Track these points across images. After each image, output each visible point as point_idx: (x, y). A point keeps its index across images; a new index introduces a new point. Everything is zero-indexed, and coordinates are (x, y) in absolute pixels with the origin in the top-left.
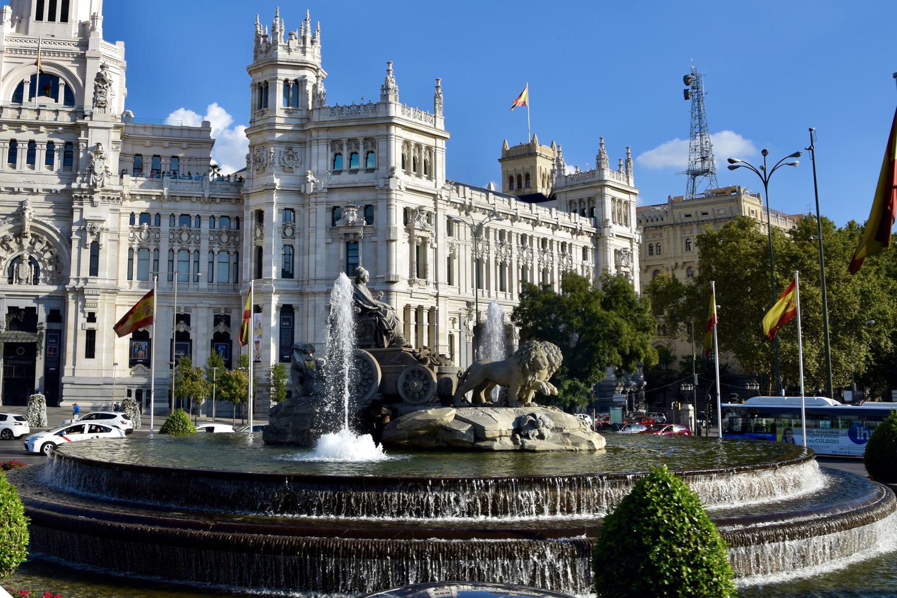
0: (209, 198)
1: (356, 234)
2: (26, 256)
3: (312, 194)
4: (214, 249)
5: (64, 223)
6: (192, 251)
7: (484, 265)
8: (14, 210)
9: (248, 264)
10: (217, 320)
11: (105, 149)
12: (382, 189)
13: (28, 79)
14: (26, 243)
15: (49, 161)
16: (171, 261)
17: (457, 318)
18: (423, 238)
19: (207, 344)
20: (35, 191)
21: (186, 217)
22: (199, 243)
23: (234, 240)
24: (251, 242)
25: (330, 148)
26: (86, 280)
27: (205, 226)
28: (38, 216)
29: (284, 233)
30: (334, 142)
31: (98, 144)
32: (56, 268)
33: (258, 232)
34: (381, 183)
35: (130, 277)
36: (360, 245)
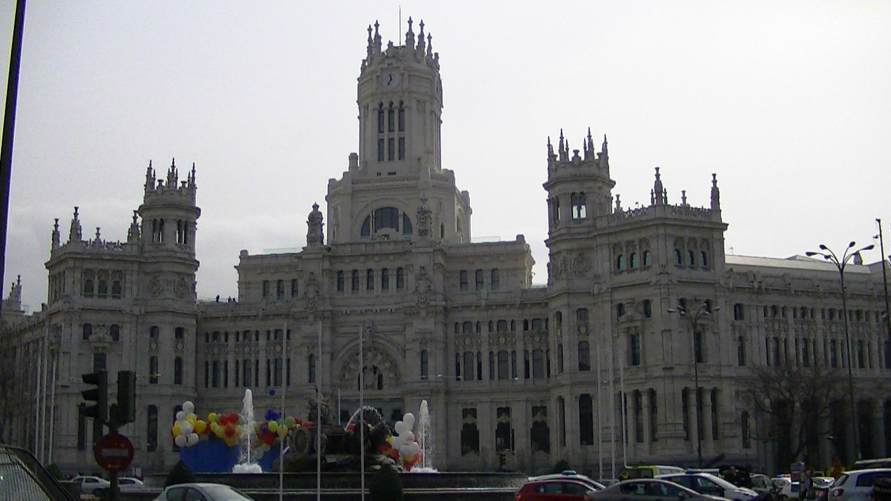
2: (370, 366)
4: (528, 349)
6: (510, 352)
9: (554, 362)
10: (535, 410)
12: (655, 285)
14: (370, 355)
16: (491, 362)
17: (752, 396)
18: (702, 325)
19: (527, 433)
21: (501, 323)
22: (515, 344)
24: (554, 341)
29: (579, 331)
32: (396, 375)
33: (559, 331)
34: (654, 280)
36: (640, 337)
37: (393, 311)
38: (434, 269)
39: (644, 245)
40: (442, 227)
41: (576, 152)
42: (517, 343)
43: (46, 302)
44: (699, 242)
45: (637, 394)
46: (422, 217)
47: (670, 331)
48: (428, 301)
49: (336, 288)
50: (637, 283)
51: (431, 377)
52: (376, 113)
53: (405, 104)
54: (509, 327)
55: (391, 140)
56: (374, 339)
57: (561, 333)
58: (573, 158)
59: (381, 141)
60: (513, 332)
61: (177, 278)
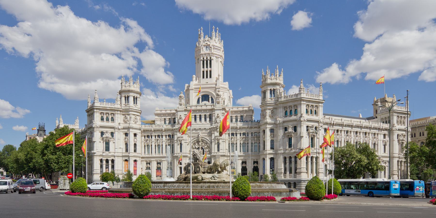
0: (251, 127)
1: (291, 135)
2: (200, 147)
3: (278, 124)
5: (210, 137)
6: (246, 143)
7: (340, 143)
8: (197, 135)
11: (220, 115)
14: (200, 143)
20: (202, 129)
23: (259, 139)
25: (284, 109)
26: (216, 153)
27: (250, 135)
30: (285, 107)
31: (218, 114)
35: (240, 151)
40: (224, 101)
42: (249, 140)
43: (87, 124)
45: (290, 158)
47: (303, 137)
51: (220, 151)
52: (202, 62)
53: (212, 58)
55: (207, 72)
56: (202, 138)
57: (265, 137)
61: (134, 116)
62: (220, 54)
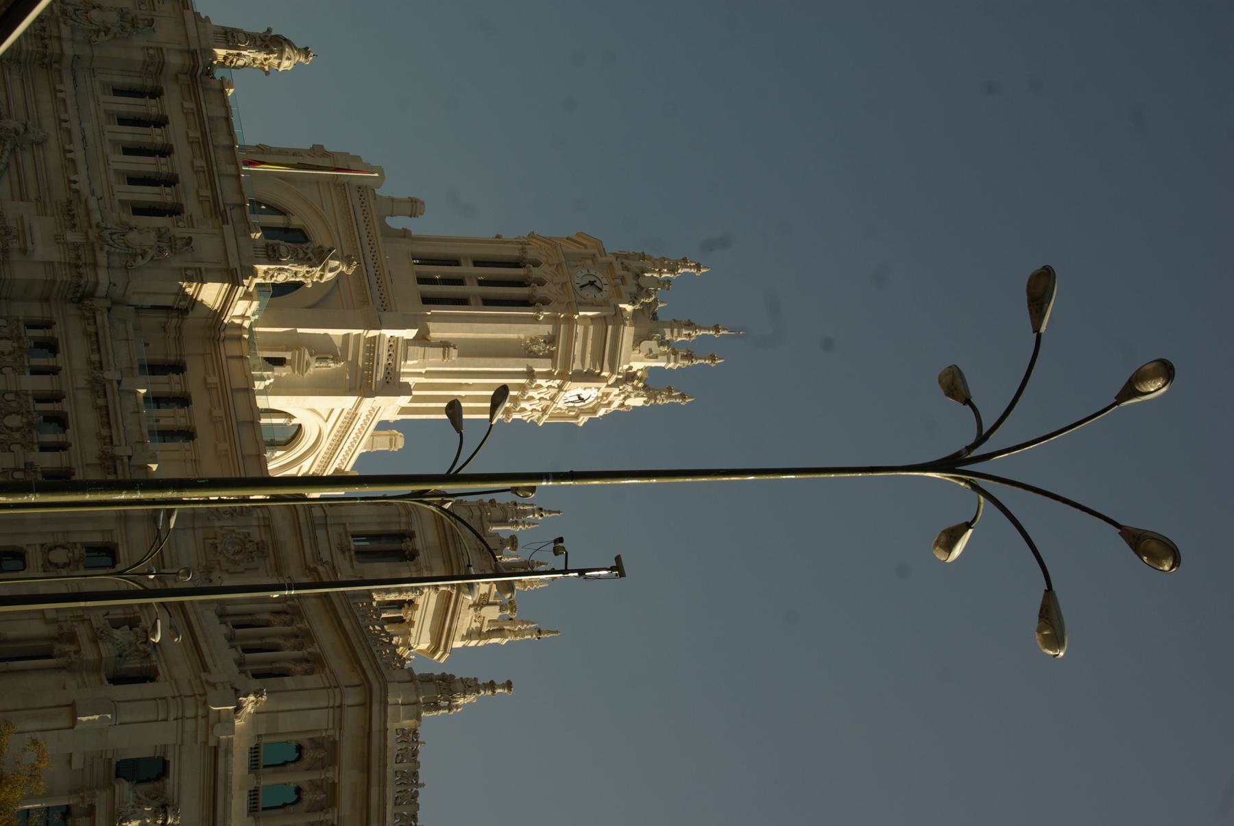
0: (114, 458)
13: (296, 222)
15: (134, 180)
21: (60, 421)
28: (13, 150)
29: (55, 547)
31: (190, 238)
37: (74, 186)
38: (186, 269)
39: (306, 666)
41: (513, 542)
44: (328, 817)
46: (309, 251)
47: (72, 727)
48: (106, 248)
49: (118, 80)
50: (204, 648)
54: (50, 438)
55: (459, 282)
58: (496, 534)
59: (456, 262)
60: (36, 448)
62: (577, 366)
